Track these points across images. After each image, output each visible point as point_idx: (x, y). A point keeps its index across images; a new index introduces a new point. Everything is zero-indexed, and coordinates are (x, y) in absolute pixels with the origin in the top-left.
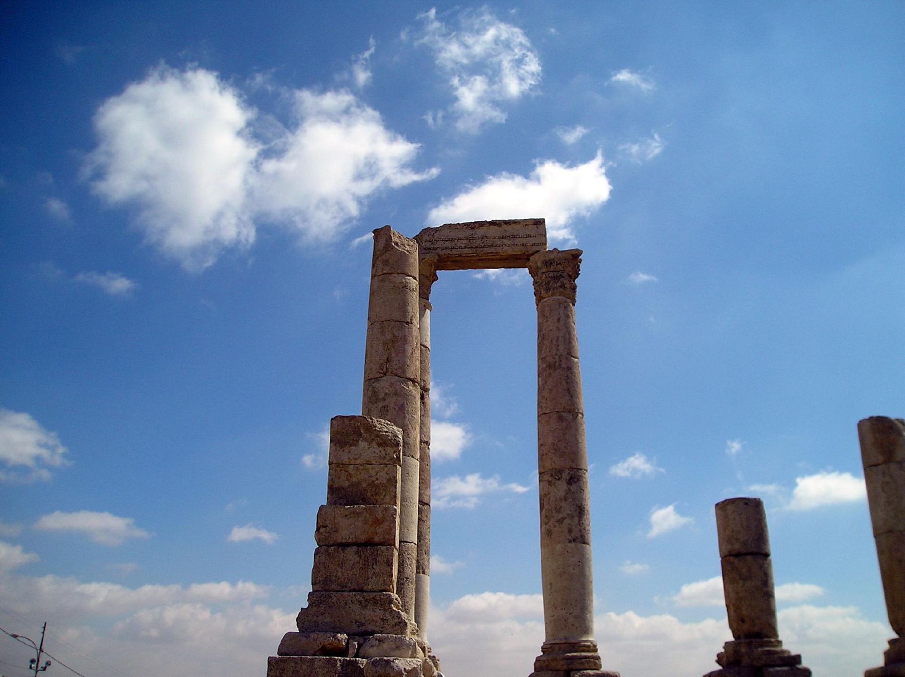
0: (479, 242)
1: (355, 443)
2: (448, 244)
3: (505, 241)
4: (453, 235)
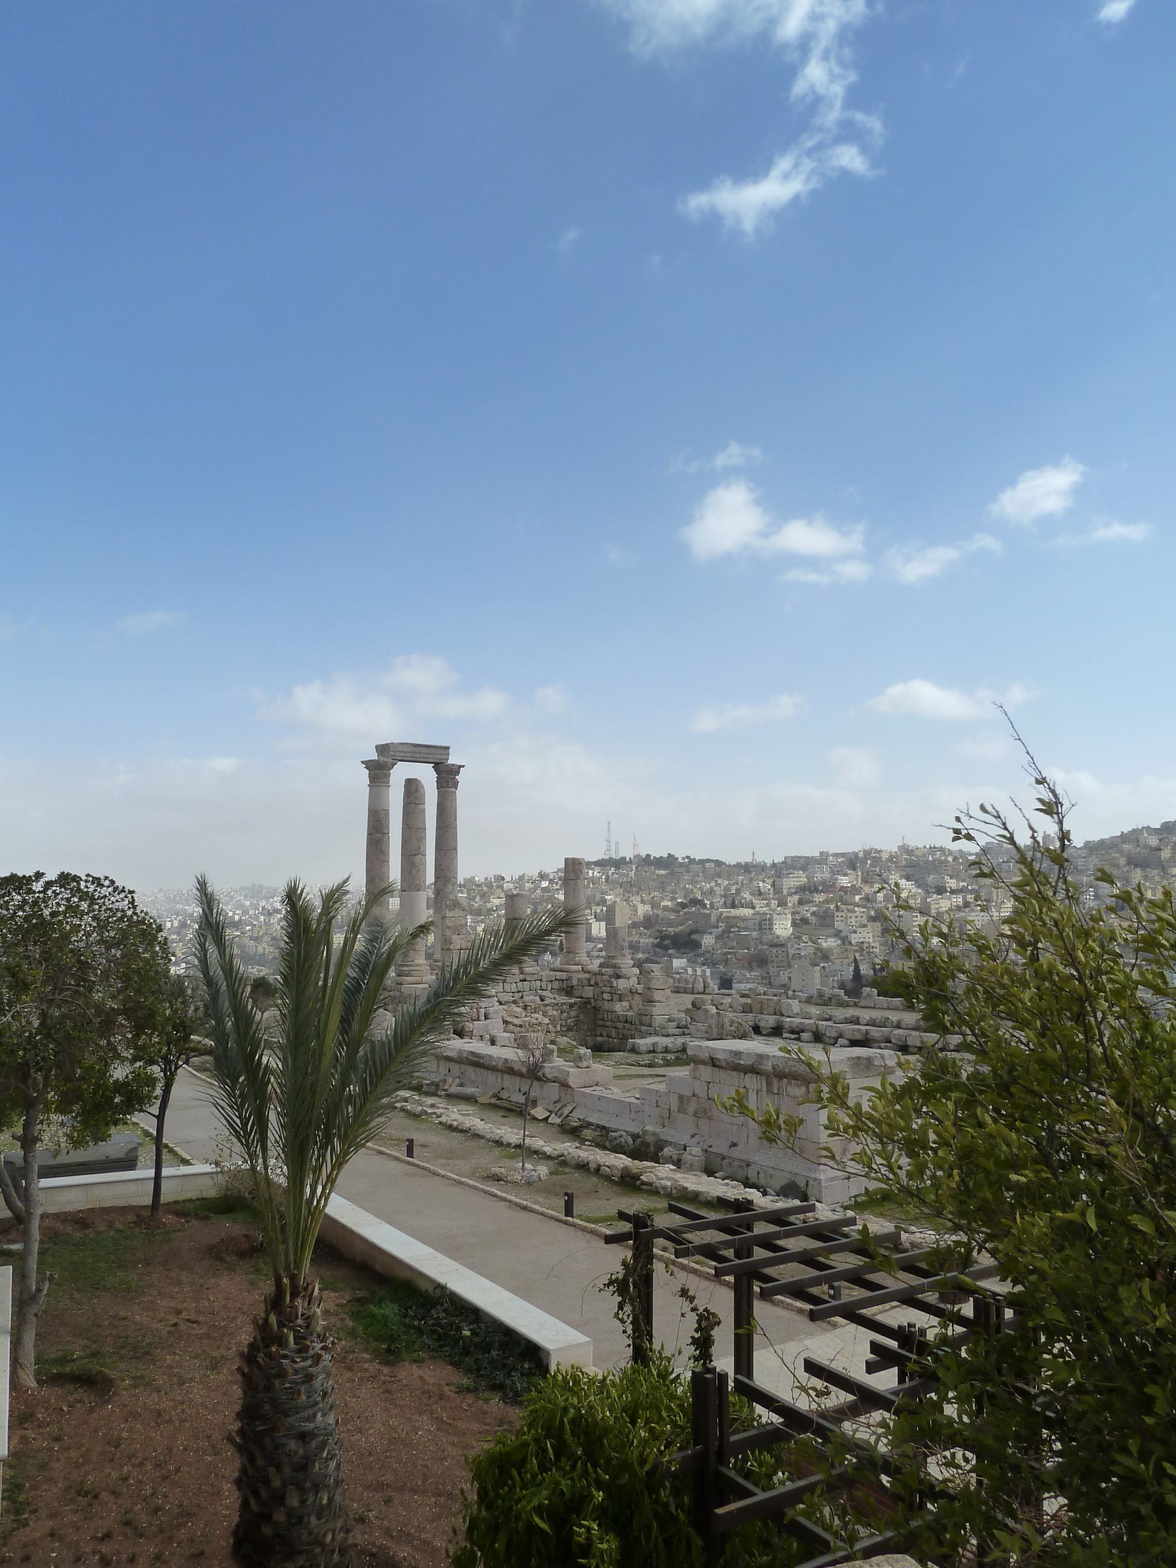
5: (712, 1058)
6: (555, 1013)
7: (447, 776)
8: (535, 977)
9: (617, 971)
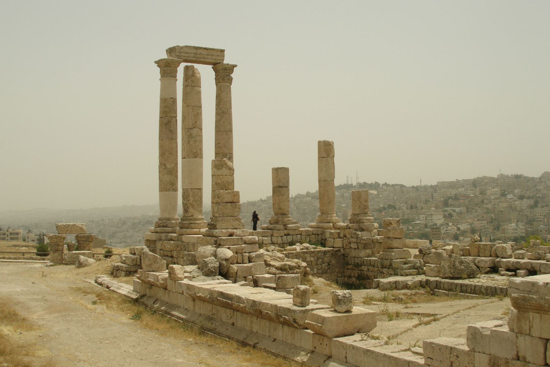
0: (199, 56)
2: (186, 55)
3: (209, 57)
4: (188, 51)
6: (312, 259)
7: (224, 74)
8: (297, 232)
9: (362, 225)
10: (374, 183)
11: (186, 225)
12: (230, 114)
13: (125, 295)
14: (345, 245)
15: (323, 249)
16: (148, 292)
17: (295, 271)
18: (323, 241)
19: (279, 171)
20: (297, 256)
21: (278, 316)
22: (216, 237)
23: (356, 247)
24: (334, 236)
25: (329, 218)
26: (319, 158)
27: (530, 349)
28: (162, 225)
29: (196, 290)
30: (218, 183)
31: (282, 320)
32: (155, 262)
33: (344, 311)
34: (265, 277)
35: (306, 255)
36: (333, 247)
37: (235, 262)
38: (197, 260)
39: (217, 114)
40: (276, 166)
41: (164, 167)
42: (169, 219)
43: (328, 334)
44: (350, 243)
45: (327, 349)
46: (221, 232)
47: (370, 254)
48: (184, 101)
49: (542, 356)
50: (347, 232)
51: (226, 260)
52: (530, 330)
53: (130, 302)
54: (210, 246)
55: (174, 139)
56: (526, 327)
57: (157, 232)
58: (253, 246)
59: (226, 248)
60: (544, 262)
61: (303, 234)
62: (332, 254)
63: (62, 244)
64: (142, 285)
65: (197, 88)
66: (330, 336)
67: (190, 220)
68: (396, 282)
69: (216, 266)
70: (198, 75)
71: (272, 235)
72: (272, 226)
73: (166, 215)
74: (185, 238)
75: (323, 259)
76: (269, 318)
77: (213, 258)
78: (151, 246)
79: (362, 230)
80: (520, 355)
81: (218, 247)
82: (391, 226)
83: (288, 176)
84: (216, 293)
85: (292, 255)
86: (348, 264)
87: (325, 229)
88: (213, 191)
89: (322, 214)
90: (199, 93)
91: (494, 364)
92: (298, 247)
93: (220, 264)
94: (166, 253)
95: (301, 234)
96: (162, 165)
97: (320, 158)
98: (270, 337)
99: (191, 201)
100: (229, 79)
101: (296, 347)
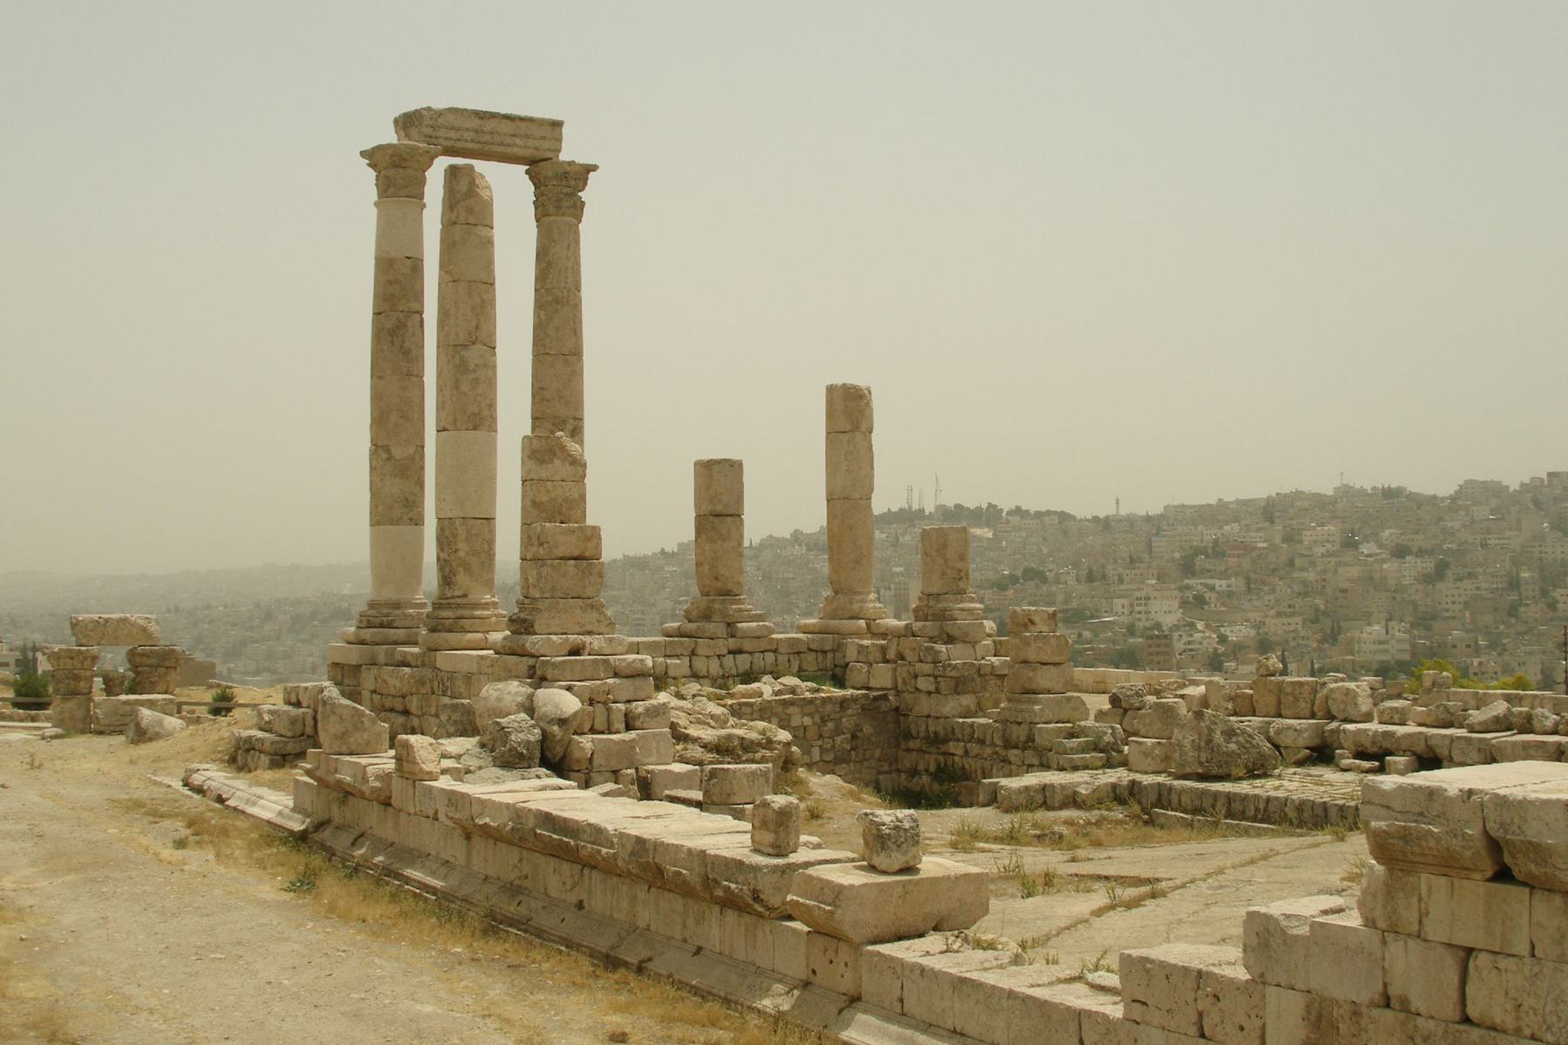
0: (487, 137)
1: (552, 461)
2: (452, 134)
3: (518, 141)
4: (458, 123)
5: (1495, 846)
6: (807, 721)
7: (560, 192)
8: (763, 644)
9: (949, 626)
10: (984, 506)
11: (447, 622)
12: (577, 307)
13: (269, 822)
14: (900, 681)
15: (838, 693)
16: (335, 813)
17: (758, 756)
18: (838, 670)
19: (716, 468)
20: (764, 711)
21: (709, 883)
22: (533, 656)
23: (932, 688)
24: (871, 658)
25: (856, 606)
26: (828, 433)
27: (1419, 975)
28: (377, 621)
29: (476, 809)
30: (541, 503)
31: (719, 893)
32: (356, 728)
33: (897, 867)
34: (671, 772)
35: (791, 710)
36: (868, 688)
37: (587, 727)
38: (479, 722)
39: (539, 305)
40: (706, 457)
41: (384, 456)
42: (397, 605)
43: (851, 934)
44: (916, 677)
45: (849, 975)
46: (547, 642)
47: (973, 707)
48: (443, 266)
49: (1455, 995)
50: (907, 644)
51: (562, 722)
52: (1420, 922)
53: (284, 842)
54: (516, 683)
55: (414, 374)
56: (1409, 916)
57: (362, 642)
58: (639, 682)
59: (561, 687)
60: (1462, 732)
61: (782, 650)
62: (863, 709)
63: (88, 673)
64: (319, 793)
65: (482, 231)
66: (857, 939)
67: (459, 606)
68: (1044, 788)
69: (532, 738)
70: (484, 194)
71: (693, 653)
72: (693, 626)
73: (390, 594)
74: (443, 659)
75: (838, 721)
76: (683, 889)
77: (523, 716)
78: (347, 681)
79: (950, 640)
80: (1394, 991)
81: (537, 686)
82: (1032, 628)
83: (741, 484)
84: (531, 816)
85: (748, 710)
86: (908, 736)
87: (844, 635)
88: (526, 524)
89: (836, 592)
90: (490, 242)
91: (1319, 1018)
92: (766, 688)
93: (544, 733)
94: (388, 703)
95: (775, 651)
96: (380, 450)
97: (833, 434)
98: (685, 941)
99: (461, 554)
100: (574, 206)
101: (759, 972)
